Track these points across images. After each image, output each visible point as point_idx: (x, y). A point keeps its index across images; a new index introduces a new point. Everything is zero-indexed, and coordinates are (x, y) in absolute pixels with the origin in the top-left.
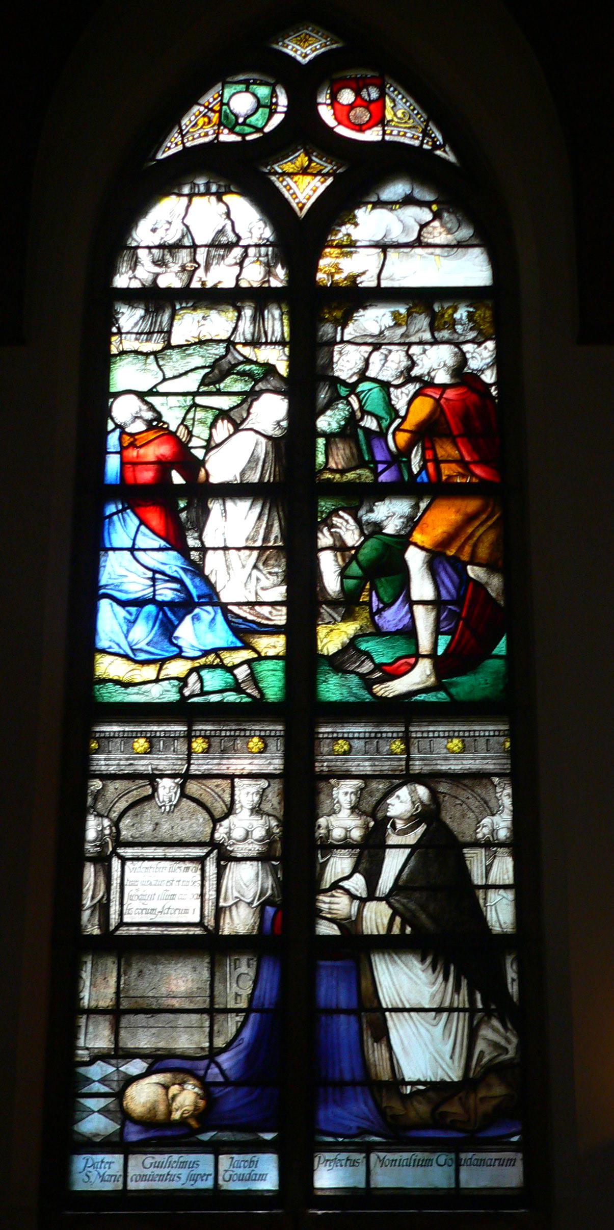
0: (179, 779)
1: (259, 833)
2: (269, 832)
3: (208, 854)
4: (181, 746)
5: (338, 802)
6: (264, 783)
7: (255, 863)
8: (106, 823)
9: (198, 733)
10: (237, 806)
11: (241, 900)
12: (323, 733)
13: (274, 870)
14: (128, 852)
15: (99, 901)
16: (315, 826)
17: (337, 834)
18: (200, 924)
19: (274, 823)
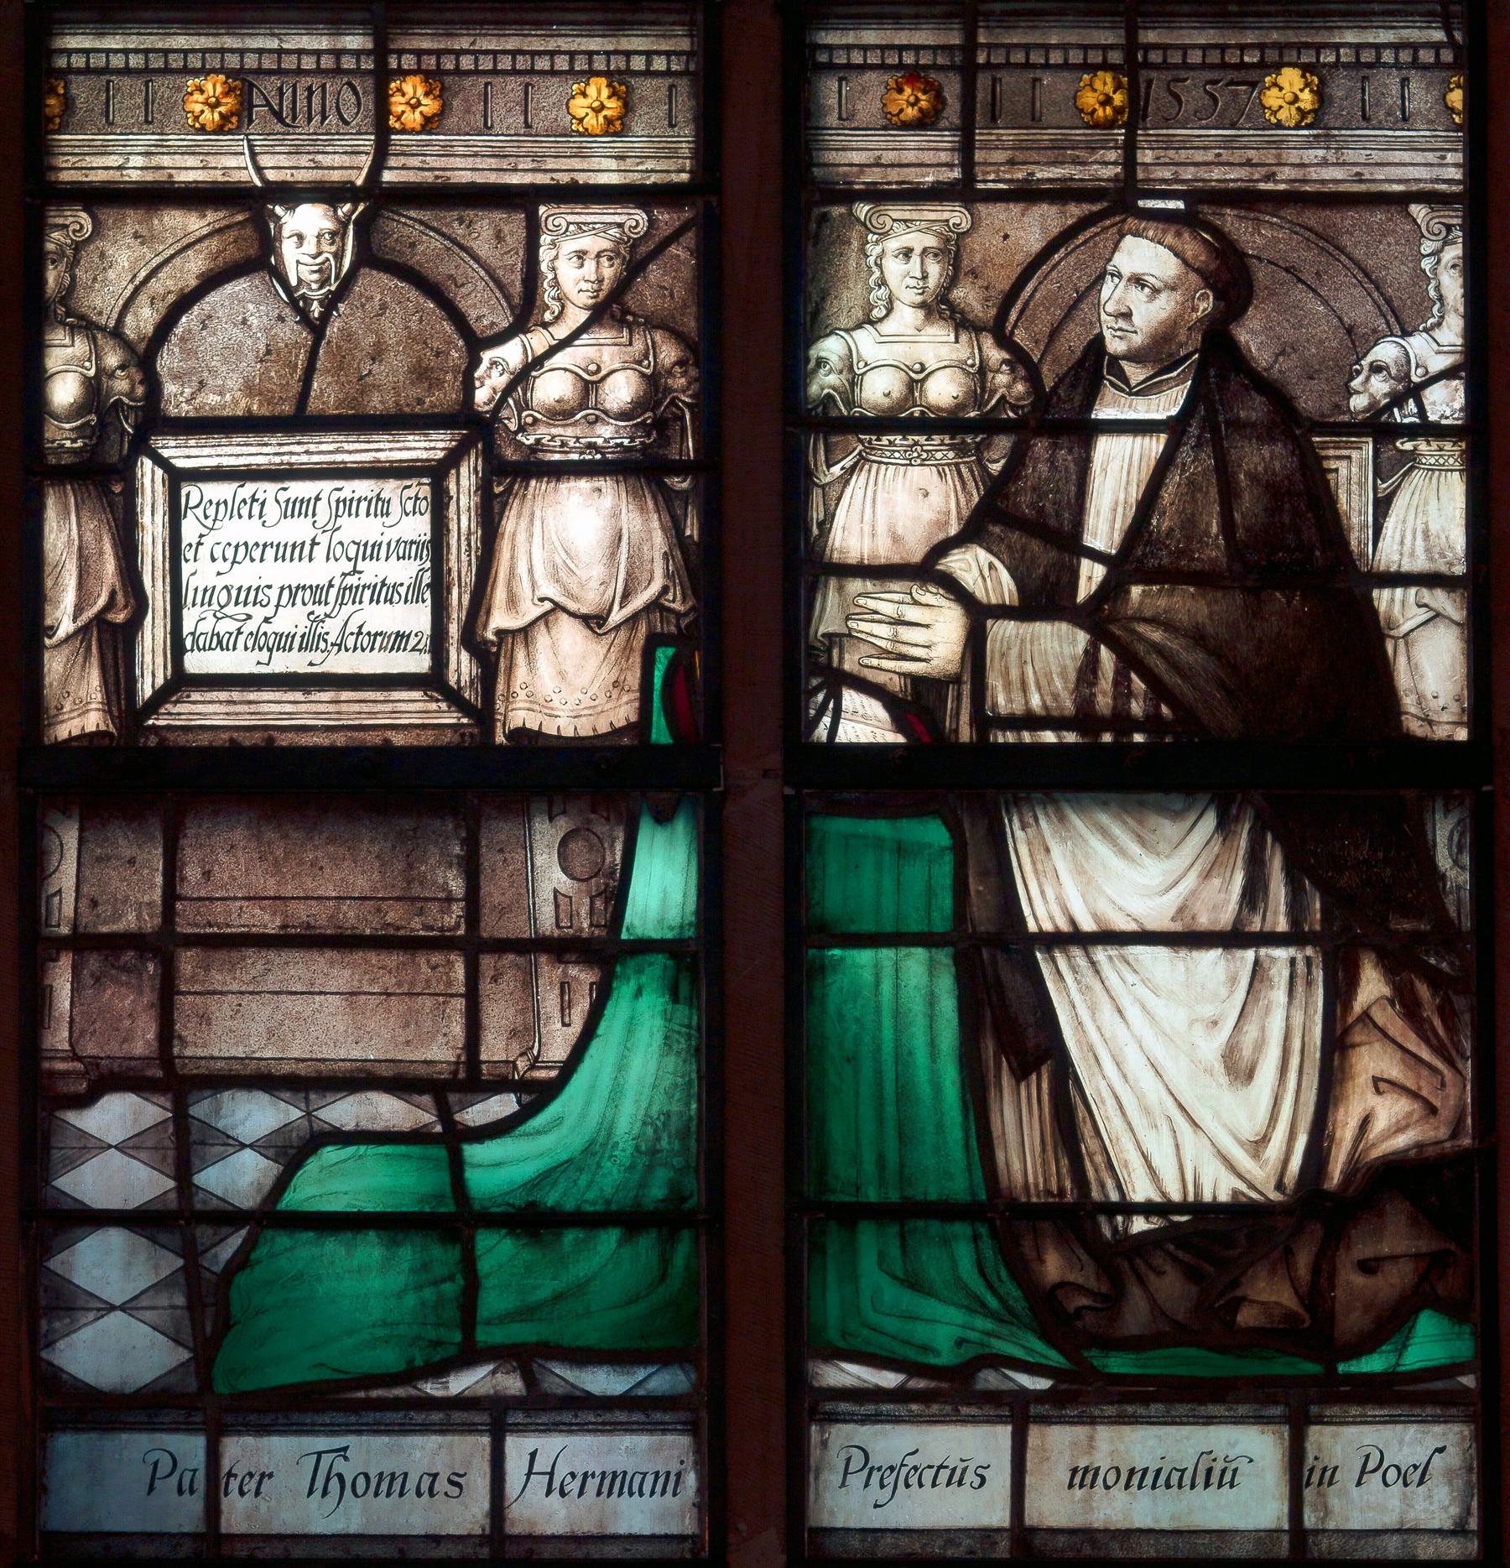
0: (347, 207)
1: (621, 390)
2: (654, 383)
3: (453, 459)
4: (353, 103)
5: (882, 282)
6: (635, 219)
7: (606, 484)
8: (112, 360)
9: (408, 62)
10: (548, 295)
11: (558, 607)
12: (830, 48)
13: (669, 503)
14: (184, 453)
15: (100, 618)
16: (808, 360)
17: (879, 389)
18: (433, 682)
19: (669, 353)
